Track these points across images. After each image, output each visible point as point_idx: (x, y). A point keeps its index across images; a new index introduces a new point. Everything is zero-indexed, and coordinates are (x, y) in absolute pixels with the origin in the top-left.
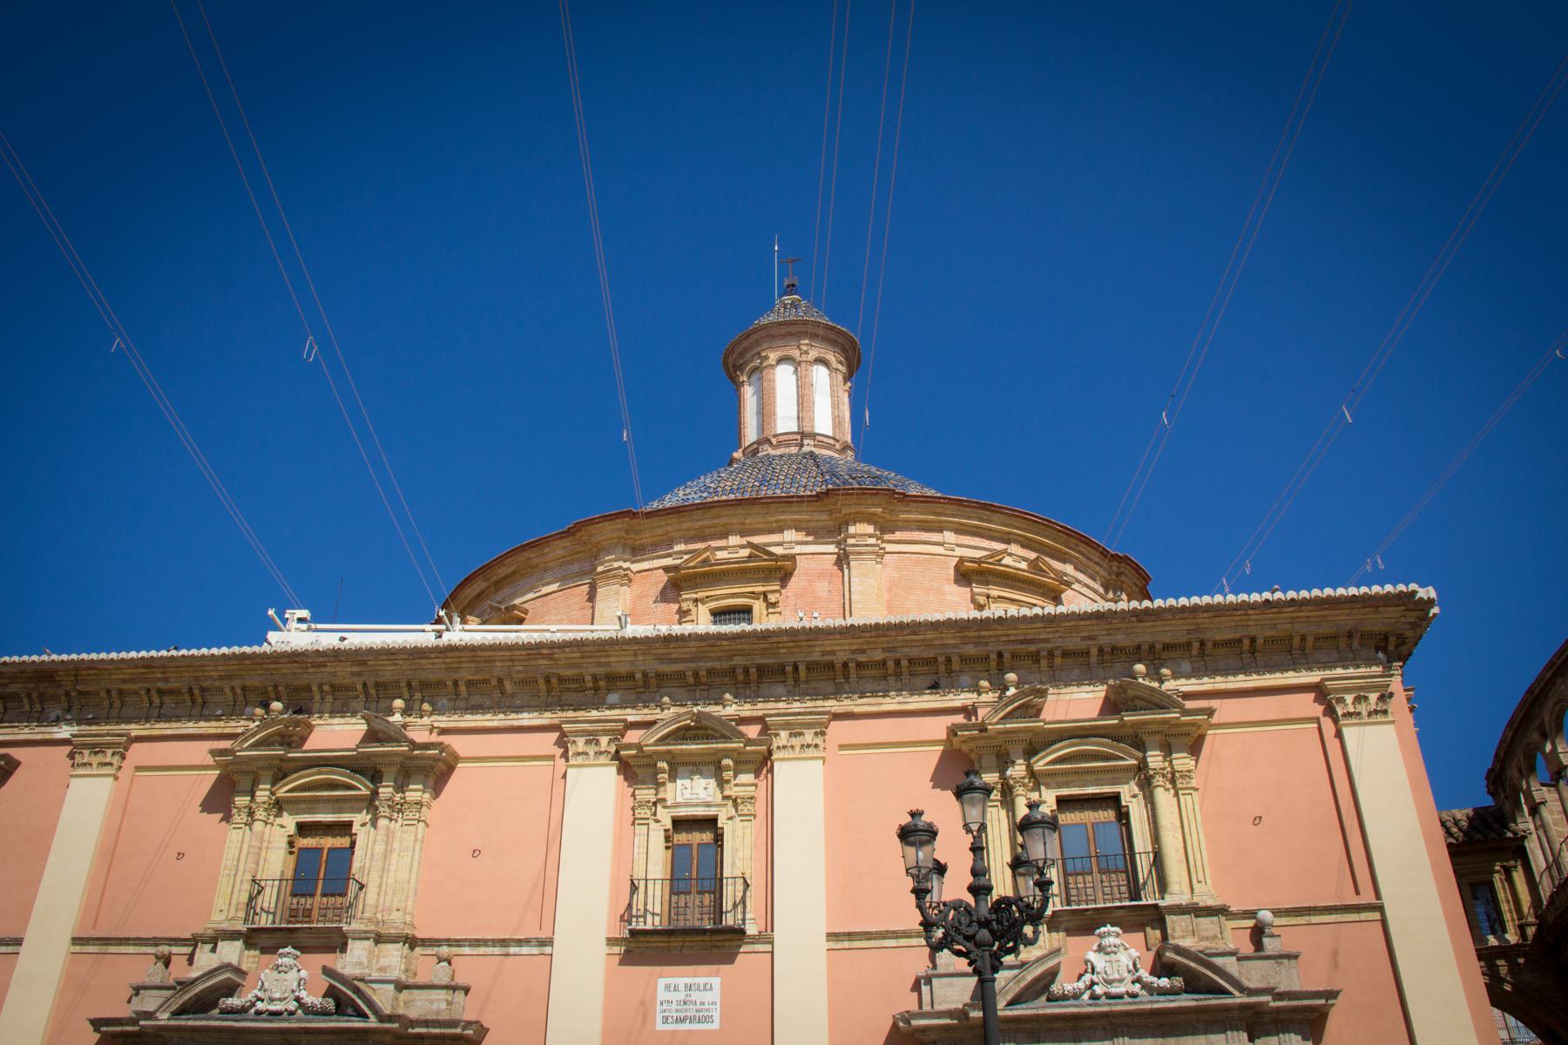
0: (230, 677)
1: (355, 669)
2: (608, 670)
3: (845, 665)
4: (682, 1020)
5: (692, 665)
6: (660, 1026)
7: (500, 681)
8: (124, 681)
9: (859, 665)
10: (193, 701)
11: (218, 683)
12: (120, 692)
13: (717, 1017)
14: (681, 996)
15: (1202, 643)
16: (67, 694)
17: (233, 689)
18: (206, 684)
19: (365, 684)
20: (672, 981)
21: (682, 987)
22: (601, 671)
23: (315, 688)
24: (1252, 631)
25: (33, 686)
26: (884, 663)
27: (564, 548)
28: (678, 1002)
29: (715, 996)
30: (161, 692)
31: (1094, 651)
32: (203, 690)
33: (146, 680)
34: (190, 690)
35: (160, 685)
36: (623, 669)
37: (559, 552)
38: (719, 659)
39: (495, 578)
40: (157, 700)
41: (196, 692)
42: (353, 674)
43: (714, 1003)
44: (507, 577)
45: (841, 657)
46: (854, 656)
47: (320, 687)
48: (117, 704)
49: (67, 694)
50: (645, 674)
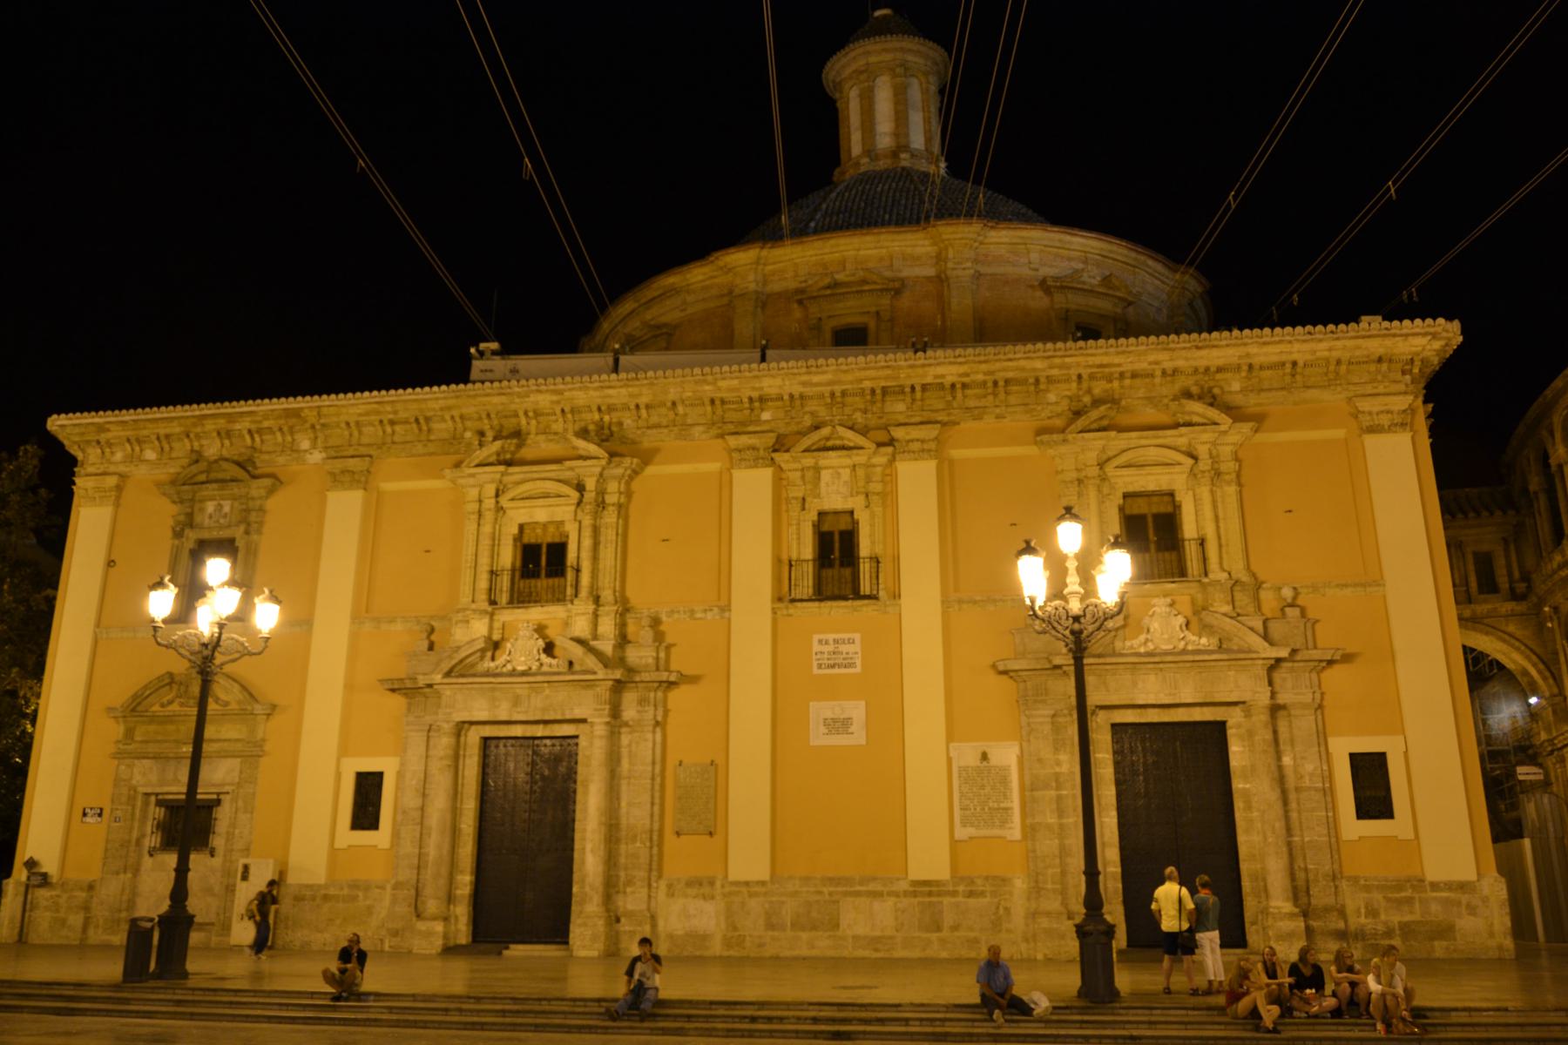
0: (449, 408)
1: (555, 398)
2: (761, 393)
3: (953, 386)
4: (833, 666)
5: (829, 388)
6: (816, 671)
7: (674, 404)
8: (360, 415)
9: (964, 386)
10: (420, 430)
11: (439, 413)
12: (358, 424)
13: (858, 662)
14: (831, 648)
15: (1250, 366)
16: (313, 427)
17: (452, 418)
18: (429, 414)
19: (563, 411)
20: (822, 636)
21: (831, 642)
22: (755, 395)
23: (521, 413)
24: (1295, 357)
26: (984, 383)
27: (704, 274)
28: (829, 653)
29: (856, 647)
30: (392, 423)
31: (1158, 373)
33: (378, 413)
34: (417, 421)
35: (391, 416)
36: (773, 391)
38: (851, 383)
40: (389, 430)
41: (422, 421)
43: (856, 653)
44: (654, 298)
45: (949, 380)
46: (960, 379)
47: (526, 413)
48: (356, 433)
49: (313, 427)
50: (791, 396)
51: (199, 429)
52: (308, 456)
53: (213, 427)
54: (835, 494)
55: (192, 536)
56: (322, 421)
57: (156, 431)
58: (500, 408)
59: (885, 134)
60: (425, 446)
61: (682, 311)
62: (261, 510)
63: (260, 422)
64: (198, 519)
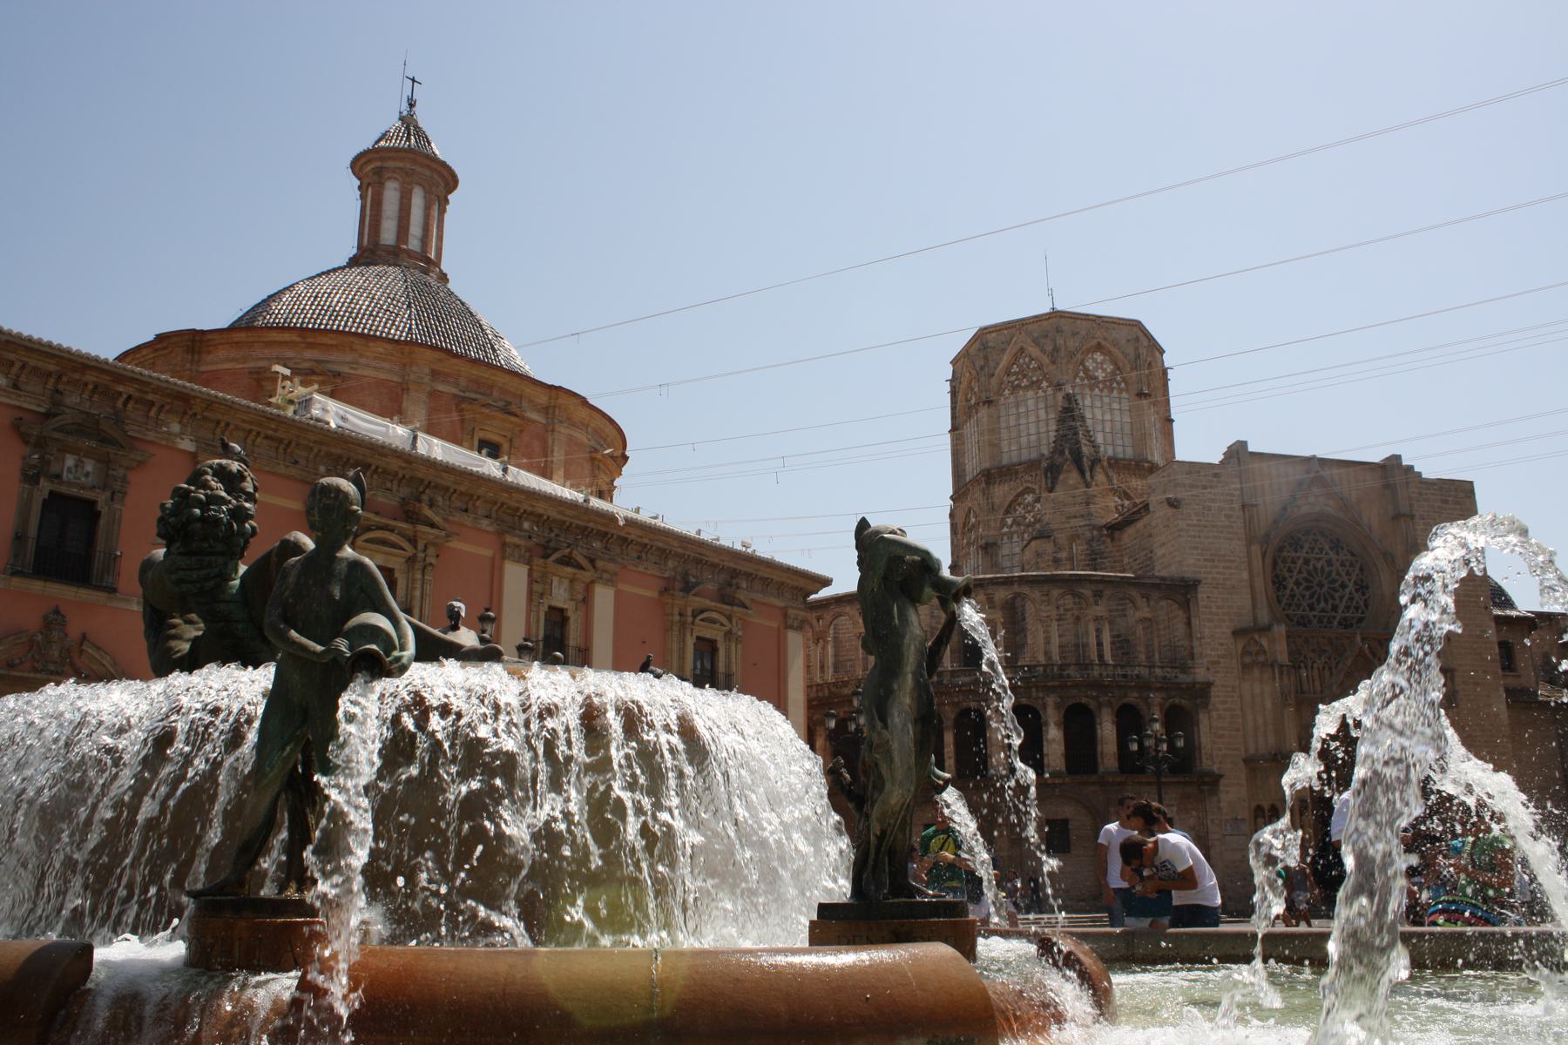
1: (404, 465)
8: (244, 421)
11: (311, 444)
22: (529, 509)
24: (774, 577)
25: (169, 400)
26: (646, 545)
27: (385, 349)
30: (267, 437)
32: (298, 445)
35: (270, 432)
37: (381, 350)
39: (311, 340)
41: (293, 445)
42: (400, 467)
45: (632, 537)
51: (77, 376)
52: (178, 440)
53: (94, 379)
54: (560, 596)
55: (45, 486)
56: (205, 414)
57: (25, 359)
58: (360, 457)
59: (415, 236)
60: (287, 467)
61: (352, 368)
62: (124, 480)
63: (146, 393)
64: (54, 469)
